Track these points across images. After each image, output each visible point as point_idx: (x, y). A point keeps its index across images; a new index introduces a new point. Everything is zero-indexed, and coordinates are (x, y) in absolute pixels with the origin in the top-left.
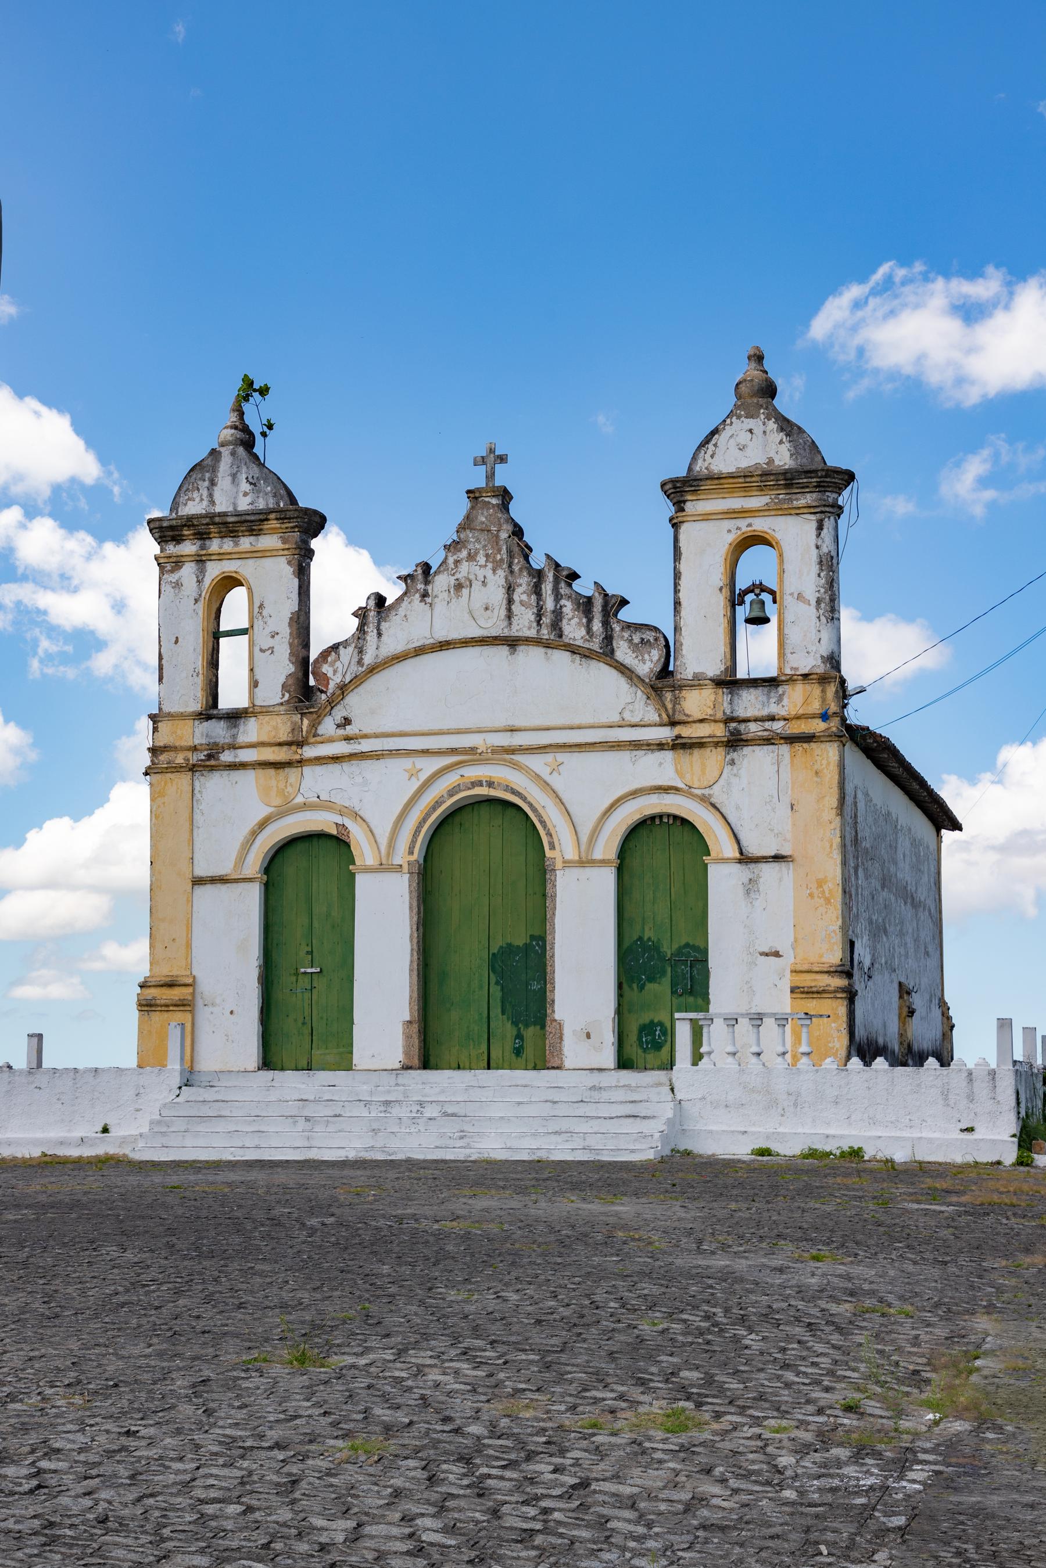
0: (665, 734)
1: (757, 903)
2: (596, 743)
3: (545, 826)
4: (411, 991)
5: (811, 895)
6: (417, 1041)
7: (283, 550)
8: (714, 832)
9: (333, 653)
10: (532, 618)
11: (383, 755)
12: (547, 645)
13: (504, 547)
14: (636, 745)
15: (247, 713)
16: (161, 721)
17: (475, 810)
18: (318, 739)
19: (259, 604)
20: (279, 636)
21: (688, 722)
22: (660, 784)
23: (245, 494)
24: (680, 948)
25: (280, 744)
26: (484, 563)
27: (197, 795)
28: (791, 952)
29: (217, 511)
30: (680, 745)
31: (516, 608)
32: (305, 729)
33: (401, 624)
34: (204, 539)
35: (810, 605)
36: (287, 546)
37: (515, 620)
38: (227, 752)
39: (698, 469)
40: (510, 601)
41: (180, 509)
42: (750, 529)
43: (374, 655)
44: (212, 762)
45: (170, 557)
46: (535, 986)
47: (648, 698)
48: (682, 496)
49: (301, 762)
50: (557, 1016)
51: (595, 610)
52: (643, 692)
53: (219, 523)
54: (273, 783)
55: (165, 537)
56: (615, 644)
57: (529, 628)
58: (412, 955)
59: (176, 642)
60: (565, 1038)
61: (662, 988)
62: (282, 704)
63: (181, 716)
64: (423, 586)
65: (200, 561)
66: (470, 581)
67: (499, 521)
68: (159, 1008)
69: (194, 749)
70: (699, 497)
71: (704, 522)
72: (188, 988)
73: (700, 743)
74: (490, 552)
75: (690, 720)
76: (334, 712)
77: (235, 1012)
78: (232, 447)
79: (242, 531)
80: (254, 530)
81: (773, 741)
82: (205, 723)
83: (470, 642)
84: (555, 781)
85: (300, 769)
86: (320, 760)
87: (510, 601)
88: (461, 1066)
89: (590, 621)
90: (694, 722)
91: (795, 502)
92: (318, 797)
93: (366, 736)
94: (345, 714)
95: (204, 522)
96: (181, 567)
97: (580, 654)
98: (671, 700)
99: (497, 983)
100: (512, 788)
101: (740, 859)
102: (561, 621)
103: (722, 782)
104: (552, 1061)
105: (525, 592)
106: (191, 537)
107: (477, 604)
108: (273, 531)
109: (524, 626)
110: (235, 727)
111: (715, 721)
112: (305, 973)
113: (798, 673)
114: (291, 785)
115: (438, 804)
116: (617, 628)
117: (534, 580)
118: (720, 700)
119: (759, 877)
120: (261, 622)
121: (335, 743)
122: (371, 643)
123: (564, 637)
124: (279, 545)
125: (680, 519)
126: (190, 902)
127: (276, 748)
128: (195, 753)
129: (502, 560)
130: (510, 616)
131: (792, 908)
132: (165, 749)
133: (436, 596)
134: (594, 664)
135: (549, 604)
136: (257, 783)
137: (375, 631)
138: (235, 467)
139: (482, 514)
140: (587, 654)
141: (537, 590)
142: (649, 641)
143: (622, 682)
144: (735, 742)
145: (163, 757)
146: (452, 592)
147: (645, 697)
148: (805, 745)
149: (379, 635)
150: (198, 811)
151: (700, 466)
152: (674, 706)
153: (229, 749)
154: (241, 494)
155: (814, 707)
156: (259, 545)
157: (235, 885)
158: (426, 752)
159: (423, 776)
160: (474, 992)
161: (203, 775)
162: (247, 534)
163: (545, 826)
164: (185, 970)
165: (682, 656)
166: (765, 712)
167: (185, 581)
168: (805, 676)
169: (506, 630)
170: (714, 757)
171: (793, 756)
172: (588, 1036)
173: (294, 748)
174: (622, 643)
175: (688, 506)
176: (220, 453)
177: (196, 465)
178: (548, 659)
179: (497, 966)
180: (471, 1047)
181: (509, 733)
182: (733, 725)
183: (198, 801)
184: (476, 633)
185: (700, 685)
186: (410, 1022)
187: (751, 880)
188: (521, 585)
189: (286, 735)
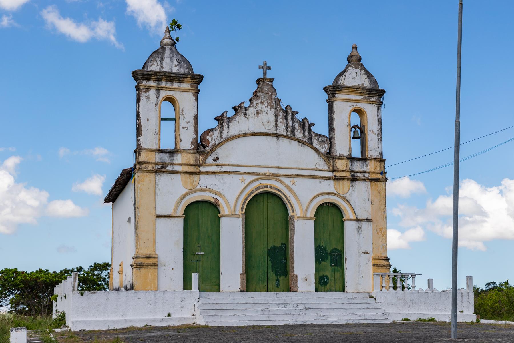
0: (330, 174)
1: (361, 235)
2: (308, 175)
3: (290, 204)
4: (243, 262)
5: (378, 233)
6: (245, 281)
7: (192, 90)
8: (347, 210)
9: (211, 132)
10: (284, 128)
11: (232, 173)
12: (290, 138)
13: (274, 101)
14: (322, 177)
15: (178, 152)
16: (142, 151)
17: (262, 196)
18: (207, 164)
20: (190, 123)
21: (339, 171)
22: (329, 191)
23: (176, 66)
24: (333, 250)
25: (191, 165)
26: (267, 106)
27: (157, 182)
28: (372, 252)
29: (164, 71)
30: (336, 179)
31: (279, 124)
32: (200, 160)
33: (237, 124)
34: (159, 81)
35: (375, 135)
36: (194, 89)
37: (278, 128)
38: (169, 166)
39: (339, 83)
40: (276, 121)
41: (148, 68)
42: (356, 106)
43: (227, 135)
44: (163, 170)
45: (146, 86)
46: (283, 262)
47: (325, 161)
48: (335, 92)
49: (200, 173)
50: (295, 273)
51: (306, 128)
52: (323, 158)
53: (167, 76)
54: (189, 180)
55: (143, 78)
56: (313, 141)
57: (283, 131)
58: (243, 249)
59: (148, 120)
60: (298, 281)
61: (326, 263)
62: (191, 150)
63: (151, 150)
64: (244, 111)
65: (158, 89)
66: (262, 112)
67: (272, 91)
68: (144, 267)
69: (156, 164)
70: (340, 93)
71: (342, 102)
72: (155, 259)
73: (343, 178)
74: (269, 102)
75: (339, 170)
76: (212, 155)
77: (174, 269)
78: (170, 47)
79: (176, 80)
80: (181, 81)
81: (366, 180)
82: (160, 154)
83: (263, 134)
84: (293, 187)
85: (199, 175)
86: (207, 173)
87: (276, 121)
88: (257, 291)
89: (304, 131)
90: (341, 171)
91: (370, 99)
92: (206, 187)
93: (225, 165)
94: (216, 156)
95: (162, 75)
96: (149, 91)
97: (301, 143)
98: (332, 163)
99: (270, 260)
100: (278, 189)
101: (356, 220)
102: (294, 130)
103: (349, 193)
104: (294, 289)
105: (281, 118)
106: (154, 80)
107: (265, 121)
108: (188, 82)
110: (172, 157)
111: (347, 171)
112: (198, 254)
113: (372, 158)
114: (196, 181)
115: (251, 193)
116: (313, 135)
117: (285, 114)
118: (348, 164)
119: (361, 226)
120: (182, 117)
122: (225, 130)
123: (295, 136)
124: (189, 88)
125: (334, 100)
126: (154, 224)
127: (189, 167)
128: (156, 165)
129: (273, 105)
130: (276, 126)
131: (372, 237)
132: (144, 163)
133: (249, 116)
134: (306, 147)
135: (290, 124)
136: (182, 179)
137: (227, 126)
138: (172, 54)
139: (266, 87)
141: (286, 118)
142: (324, 141)
143: (315, 154)
144: (354, 179)
145: (143, 166)
147: (323, 160)
148: (375, 182)
149: (229, 127)
151: (340, 82)
152: (333, 165)
153: (170, 165)
154: (174, 66)
155: (377, 169)
156: (182, 87)
157: (173, 219)
158: (248, 173)
159: (247, 182)
160: (262, 263)
161: (159, 175)
162: (177, 81)
163: (290, 204)
164: (153, 251)
165: (335, 148)
166: (362, 170)
167: (151, 96)
168: (375, 159)
169: (275, 131)
170: (347, 184)
171: (372, 186)
172: (306, 280)
173: (197, 167)
174: (315, 140)
175: (337, 96)
176: (165, 48)
177: (155, 51)
178: (290, 143)
179: (270, 254)
180: (261, 283)
181: (277, 169)
182: (352, 173)
183: (157, 185)
184: (263, 130)
185: (342, 158)
186: (243, 274)
187: (359, 227)
188: (280, 115)
189: (193, 162)
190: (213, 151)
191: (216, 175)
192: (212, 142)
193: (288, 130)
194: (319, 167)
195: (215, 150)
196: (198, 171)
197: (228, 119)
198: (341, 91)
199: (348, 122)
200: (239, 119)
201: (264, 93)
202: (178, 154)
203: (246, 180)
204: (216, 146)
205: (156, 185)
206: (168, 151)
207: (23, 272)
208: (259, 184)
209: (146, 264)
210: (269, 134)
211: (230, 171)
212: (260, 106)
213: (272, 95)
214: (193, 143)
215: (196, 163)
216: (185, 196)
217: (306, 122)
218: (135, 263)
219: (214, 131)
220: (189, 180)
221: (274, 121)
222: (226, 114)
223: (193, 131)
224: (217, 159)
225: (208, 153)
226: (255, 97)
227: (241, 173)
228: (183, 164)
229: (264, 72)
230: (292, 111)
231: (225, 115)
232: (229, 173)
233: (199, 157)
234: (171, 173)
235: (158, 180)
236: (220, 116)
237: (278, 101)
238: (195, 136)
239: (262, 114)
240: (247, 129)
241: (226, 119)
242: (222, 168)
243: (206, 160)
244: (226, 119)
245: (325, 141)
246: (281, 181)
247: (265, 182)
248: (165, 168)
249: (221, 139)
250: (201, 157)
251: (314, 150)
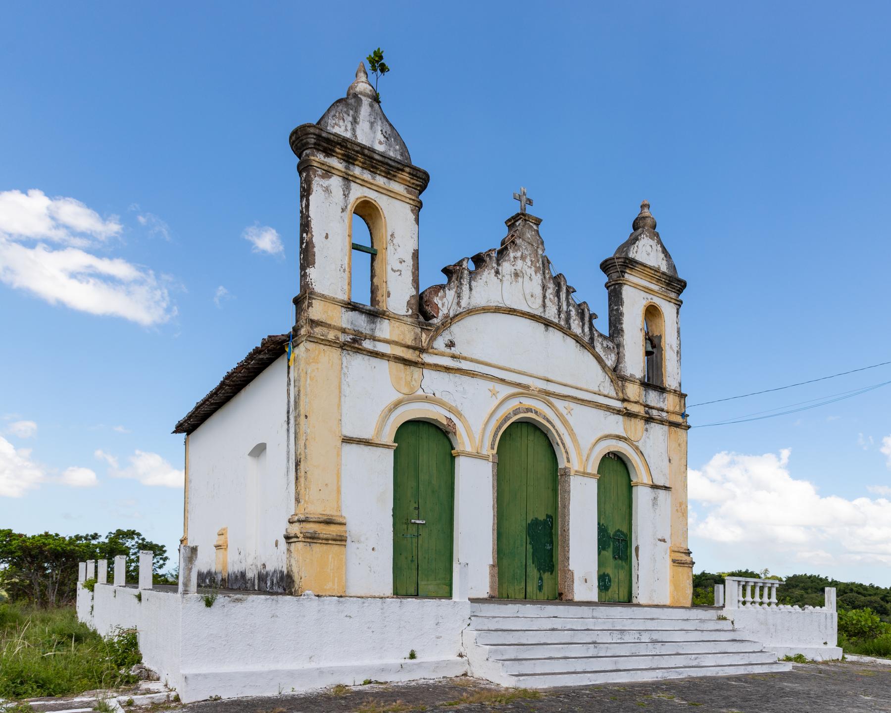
2: (591, 401)
9: (442, 291)
10: (556, 312)
13: (541, 260)
15: (384, 315)
25: (408, 347)
26: (530, 266)
27: (345, 369)
32: (423, 341)
33: (483, 286)
37: (547, 309)
40: (544, 297)
43: (467, 302)
47: (612, 381)
49: (423, 365)
52: (609, 377)
54: (403, 375)
56: (595, 342)
62: (407, 316)
64: (496, 266)
66: (523, 274)
83: (526, 314)
85: (421, 369)
86: (437, 367)
87: (544, 297)
89: (583, 325)
94: (450, 338)
105: (551, 294)
109: (552, 315)
110: (373, 323)
115: (507, 419)
122: (466, 293)
129: (539, 267)
130: (544, 306)
133: (503, 276)
135: (564, 307)
137: (468, 285)
140: (584, 345)
146: (513, 277)
147: (610, 380)
149: (471, 289)
150: (345, 383)
153: (370, 339)
161: (349, 354)
165: (625, 362)
173: (417, 352)
174: (598, 344)
178: (564, 341)
181: (546, 382)
183: (345, 374)
188: (549, 288)
189: (411, 340)
194: (604, 390)
195: (449, 327)
196: (420, 360)
197: (470, 273)
199: (642, 324)
200: (487, 278)
201: (525, 241)
202: (383, 320)
204: (451, 319)
205: (343, 375)
206: (367, 310)
207: (20, 536)
208: (518, 405)
209: (325, 536)
212: (519, 263)
213: (538, 248)
214: (410, 304)
215: (416, 344)
216: (396, 406)
217: (586, 310)
218: (301, 533)
219: (447, 291)
220: (404, 375)
221: (541, 296)
222: (467, 263)
224: (451, 344)
225: (438, 329)
226: (512, 244)
228: (393, 341)
229: (521, 206)
230: (567, 286)
231: (465, 264)
232: (473, 374)
233: (421, 334)
234: (370, 356)
235: (346, 365)
236: (455, 265)
237: (546, 263)
238: (414, 293)
239: (523, 278)
240: (500, 300)
241: (466, 272)
242: (460, 362)
243: (434, 343)
244: (466, 272)
245: (611, 347)
246: (551, 404)
247: (528, 402)
248: (359, 341)
249: (459, 308)
250: (424, 335)
251: (597, 360)
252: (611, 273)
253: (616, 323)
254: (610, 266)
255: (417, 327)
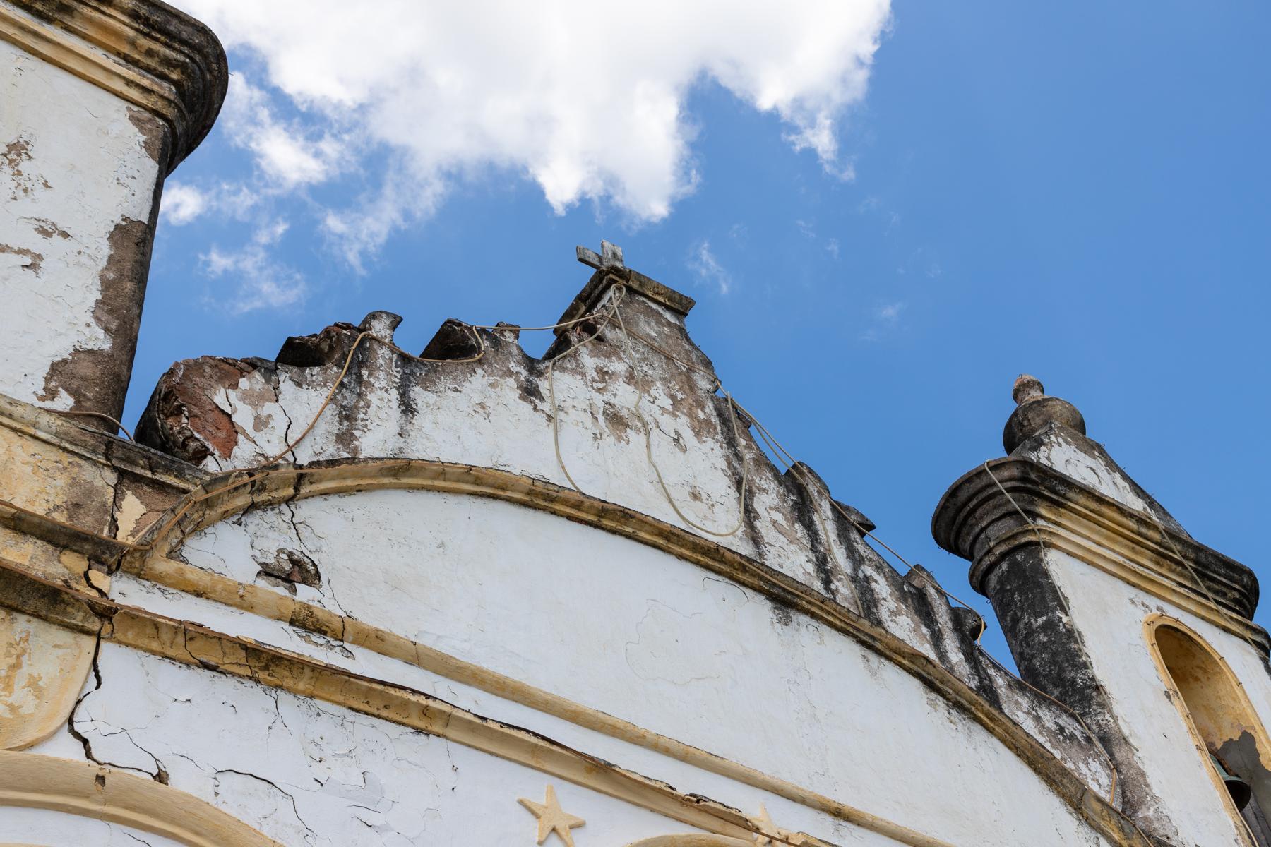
7: (129, 83)
11: (448, 719)
19: (12, 140)
48: (1032, 502)
70: (1059, 520)
94: (294, 546)
97: (944, 695)
105: (776, 509)
121: (247, 615)
122: (382, 414)
137: (394, 394)
190: (264, 497)
191: (282, 695)
192: (258, 436)
193: (833, 587)
198: (1062, 510)
203: (579, 825)
210: (722, 560)
211: (428, 697)
214: (73, 376)
223: (93, 304)
227: (536, 746)
242: (349, 654)
251: (1037, 771)
252: (984, 529)
253: (1062, 670)
254: (974, 502)
255: (94, 463)
